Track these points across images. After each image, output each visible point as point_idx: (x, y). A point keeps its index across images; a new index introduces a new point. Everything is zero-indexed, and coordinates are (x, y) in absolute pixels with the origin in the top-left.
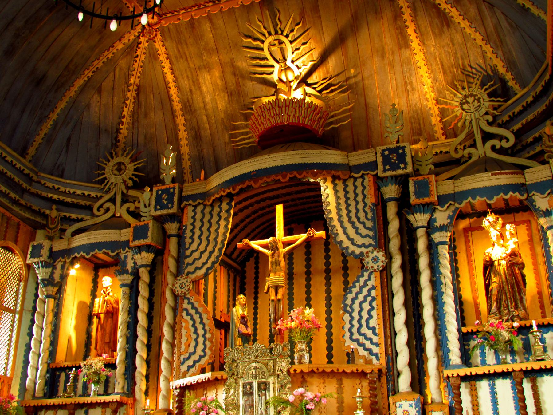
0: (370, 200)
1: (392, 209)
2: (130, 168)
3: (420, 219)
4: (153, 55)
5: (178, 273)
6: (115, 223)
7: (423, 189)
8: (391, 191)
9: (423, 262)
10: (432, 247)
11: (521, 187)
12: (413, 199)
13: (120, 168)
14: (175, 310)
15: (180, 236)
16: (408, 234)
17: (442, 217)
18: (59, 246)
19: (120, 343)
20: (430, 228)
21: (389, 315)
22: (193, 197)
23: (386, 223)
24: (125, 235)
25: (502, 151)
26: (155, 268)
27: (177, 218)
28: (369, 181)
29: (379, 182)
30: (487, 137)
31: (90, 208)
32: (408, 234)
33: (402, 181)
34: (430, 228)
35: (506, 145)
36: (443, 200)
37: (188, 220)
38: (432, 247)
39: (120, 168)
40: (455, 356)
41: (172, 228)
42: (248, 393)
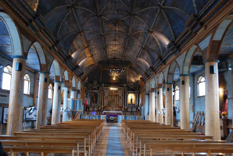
0: (122, 92)
1: (124, 93)
2: (96, 82)
3: (126, 94)
4: (101, 71)
5: (104, 96)
6: (95, 89)
7: (127, 92)
8: (124, 91)
9: (126, 98)
13: (95, 82)
15: (104, 92)
16: (125, 95)
18: (90, 91)
19: (98, 102)
22: (106, 89)
24: (98, 91)
25: (133, 88)
26: (101, 95)
27: (104, 91)
28: (122, 90)
29: (123, 91)
30: (132, 86)
31: (92, 86)
32: (125, 95)
33: (125, 91)
35: (134, 87)
37: (105, 91)
39: (95, 82)
40: (127, 106)
41: (103, 91)
42: (112, 108)
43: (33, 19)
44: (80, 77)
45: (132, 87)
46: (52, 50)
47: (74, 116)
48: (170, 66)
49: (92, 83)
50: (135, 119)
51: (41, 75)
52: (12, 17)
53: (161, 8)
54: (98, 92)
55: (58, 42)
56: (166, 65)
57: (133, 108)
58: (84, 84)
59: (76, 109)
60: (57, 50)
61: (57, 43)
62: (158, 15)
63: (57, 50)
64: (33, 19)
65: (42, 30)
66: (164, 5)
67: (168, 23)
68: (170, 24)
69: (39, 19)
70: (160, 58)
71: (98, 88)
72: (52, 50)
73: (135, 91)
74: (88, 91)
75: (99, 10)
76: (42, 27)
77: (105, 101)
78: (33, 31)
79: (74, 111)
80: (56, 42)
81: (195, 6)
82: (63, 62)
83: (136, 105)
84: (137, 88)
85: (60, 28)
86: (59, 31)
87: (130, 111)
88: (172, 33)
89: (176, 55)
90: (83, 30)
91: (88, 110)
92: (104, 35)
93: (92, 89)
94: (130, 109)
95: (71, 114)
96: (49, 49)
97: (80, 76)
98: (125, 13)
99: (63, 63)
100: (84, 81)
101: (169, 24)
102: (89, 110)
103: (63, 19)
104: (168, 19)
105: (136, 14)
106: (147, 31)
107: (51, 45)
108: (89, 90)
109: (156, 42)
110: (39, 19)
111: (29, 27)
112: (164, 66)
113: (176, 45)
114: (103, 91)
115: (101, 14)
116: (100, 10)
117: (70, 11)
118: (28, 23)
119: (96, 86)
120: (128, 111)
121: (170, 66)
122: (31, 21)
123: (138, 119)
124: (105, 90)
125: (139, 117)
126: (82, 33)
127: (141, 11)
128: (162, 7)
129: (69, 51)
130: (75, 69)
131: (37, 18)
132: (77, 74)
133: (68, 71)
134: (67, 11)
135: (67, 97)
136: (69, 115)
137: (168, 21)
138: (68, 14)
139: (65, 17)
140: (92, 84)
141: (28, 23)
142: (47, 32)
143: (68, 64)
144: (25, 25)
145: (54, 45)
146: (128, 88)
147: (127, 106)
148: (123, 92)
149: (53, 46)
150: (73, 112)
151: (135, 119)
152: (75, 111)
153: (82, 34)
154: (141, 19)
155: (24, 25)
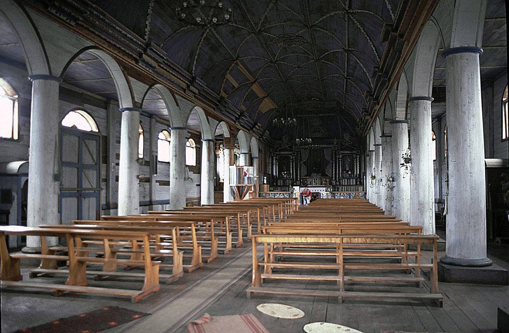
8: (334, 152)
10: (339, 161)
11: (352, 154)
12: (337, 154)
14: (300, 166)
16: (336, 158)
17: (341, 156)
20: (339, 158)
21: (332, 170)
23: (333, 156)
24: (290, 153)
26: (295, 158)
32: (336, 158)
34: (339, 158)
36: (341, 154)
38: (339, 161)
40: (341, 176)
42: (314, 180)
43: (143, 52)
44: (254, 132)
45: (347, 144)
46: (187, 91)
47: (241, 192)
48: (385, 106)
49: (281, 139)
50: (350, 197)
51: (173, 133)
52: (111, 53)
53: (348, 13)
54: (291, 154)
55: (194, 78)
56: (380, 104)
57: (350, 179)
58: (265, 141)
59: (243, 183)
60: (196, 91)
61: (192, 81)
62: (348, 24)
63: (196, 91)
64: (143, 52)
65: (162, 65)
66: (350, 7)
67: (366, 36)
68: (369, 37)
69: (151, 49)
70: (370, 93)
71: (291, 147)
72: (187, 91)
73: (353, 150)
74: (274, 154)
75: (254, 23)
76: (160, 60)
77: (302, 168)
78: (148, 69)
79: (240, 185)
80: (192, 80)
81: (389, 7)
82: (214, 108)
83: (356, 175)
84: (357, 145)
85: (196, 57)
86: (195, 62)
87: (346, 184)
88: (375, 52)
89: (386, 89)
90: (238, 56)
91: (275, 184)
92: (277, 61)
93: (280, 151)
94: (346, 180)
95: (236, 190)
96: (183, 93)
97: (252, 129)
98: (299, 24)
99: (213, 111)
100: (263, 138)
101: (368, 38)
102: (277, 184)
103: (199, 44)
104: (364, 30)
105: (315, 25)
106: (342, 50)
107: (184, 86)
108: (276, 151)
109: (362, 68)
110: (151, 49)
111: (140, 64)
112: (377, 107)
113: (383, 71)
114: (299, 153)
115: (259, 30)
116: (256, 24)
117: (208, 30)
118: (138, 58)
119: (287, 144)
120: (342, 185)
121: (385, 106)
122: (140, 55)
123: (355, 197)
124: (302, 150)
125: (357, 194)
126: (238, 61)
127: (321, 19)
128: (349, 11)
129: (221, 91)
130: (239, 119)
131: (148, 50)
132: (246, 126)
133: (227, 123)
134: (203, 31)
135: (229, 164)
136: (233, 192)
137: (365, 33)
138: (205, 35)
139: (202, 40)
140: (280, 142)
141: (138, 58)
142: (172, 66)
143: (223, 111)
144: (133, 62)
145: (189, 84)
146: (342, 145)
147: (341, 176)
148: (332, 153)
149: (188, 86)
150: (238, 187)
151: (350, 197)
152: (243, 186)
153: (239, 63)
154: (327, 32)
155: (132, 63)
